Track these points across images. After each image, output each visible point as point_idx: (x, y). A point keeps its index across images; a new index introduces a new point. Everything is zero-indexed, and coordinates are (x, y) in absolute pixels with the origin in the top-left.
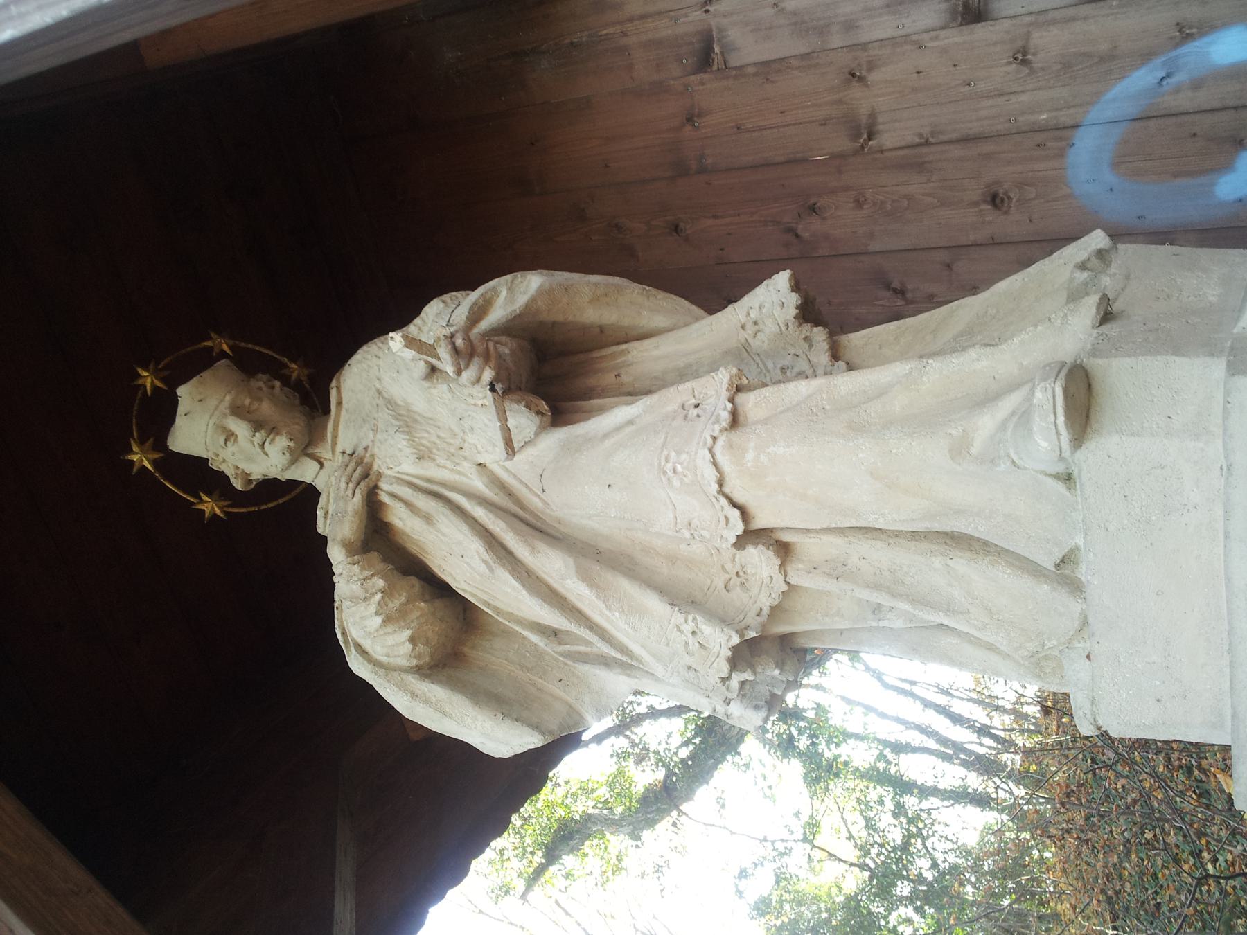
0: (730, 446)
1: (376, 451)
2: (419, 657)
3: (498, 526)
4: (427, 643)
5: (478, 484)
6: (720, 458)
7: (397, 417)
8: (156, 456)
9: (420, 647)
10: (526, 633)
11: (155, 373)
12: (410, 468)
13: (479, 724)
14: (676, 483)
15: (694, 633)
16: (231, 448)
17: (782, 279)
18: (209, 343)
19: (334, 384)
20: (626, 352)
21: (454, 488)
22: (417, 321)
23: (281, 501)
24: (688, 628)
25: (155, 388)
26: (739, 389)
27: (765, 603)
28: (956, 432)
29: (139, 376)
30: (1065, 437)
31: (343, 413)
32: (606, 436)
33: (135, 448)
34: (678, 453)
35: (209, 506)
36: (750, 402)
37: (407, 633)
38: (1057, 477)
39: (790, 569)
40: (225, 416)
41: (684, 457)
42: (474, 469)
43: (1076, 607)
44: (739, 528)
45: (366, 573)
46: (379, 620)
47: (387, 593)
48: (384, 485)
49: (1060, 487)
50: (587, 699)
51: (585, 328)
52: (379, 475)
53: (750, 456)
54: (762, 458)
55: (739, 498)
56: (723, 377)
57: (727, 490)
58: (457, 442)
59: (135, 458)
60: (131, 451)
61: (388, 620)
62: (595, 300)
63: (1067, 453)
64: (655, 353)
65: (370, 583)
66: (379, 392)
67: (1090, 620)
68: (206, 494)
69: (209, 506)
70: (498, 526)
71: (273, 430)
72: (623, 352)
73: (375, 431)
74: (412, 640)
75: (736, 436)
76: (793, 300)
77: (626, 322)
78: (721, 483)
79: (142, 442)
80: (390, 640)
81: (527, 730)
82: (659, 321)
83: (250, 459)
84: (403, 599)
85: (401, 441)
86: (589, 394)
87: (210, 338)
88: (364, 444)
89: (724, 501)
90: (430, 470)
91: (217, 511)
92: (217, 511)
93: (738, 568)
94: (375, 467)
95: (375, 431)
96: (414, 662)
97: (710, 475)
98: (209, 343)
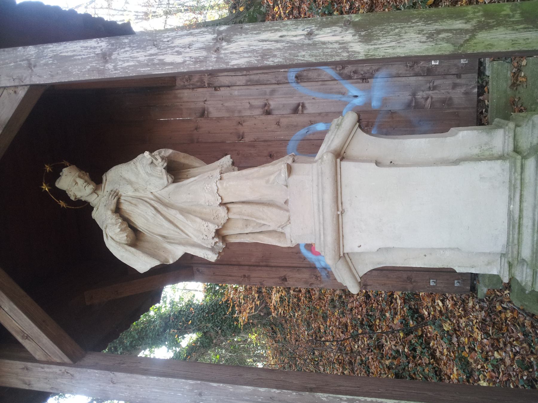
0: (220, 183)
1: (120, 190)
2: (127, 241)
3: (156, 205)
4: (130, 238)
5: (152, 197)
6: (218, 185)
7: (127, 182)
8: (50, 188)
9: (128, 239)
10: (157, 237)
11: (50, 167)
12: (130, 193)
13: (143, 258)
14: (207, 191)
15: (207, 226)
16: (76, 187)
17: (228, 157)
18: (63, 163)
19: (104, 175)
20: (189, 171)
21: (144, 197)
22: (136, 158)
23: (81, 207)
24: (205, 225)
25: (49, 171)
26: (221, 173)
27: (223, 222)
28: (267, 179)
29: (45, 167)
30: (287, 176)
31: (107, 182)
32: (188, 184)
33: (44, 185)
34: (208, 184)
35: (62, 204)
36: (224, 175)
37: (126, 234)
38: (285, 185)
39: (229, 214)
40: (77, 177)
41: (209, 185)
42: (150, 193)
43: (287, 214)
44: (220, 201)
45: (116, 218)
46: (119, 230)
47: (122, 223)
48: (122, 198)
49: (285, 187)
50: (170, 256)
51: (181, 163)
52: (121, 195)
53: (225, 185)
54: (227, 185)
55: (221, 195)
56: (218, 171)
57: (218, 192)
58: (145, 187)
59: (44, 187)
60: (42, 185)
61: (121, 230)
62: (184, 157)
63: (287, 178)
64: (197, 171)
65: (117, 220)
66: (121, 176)
67: (292, 221)
68: (61, 201)
69: (62, 204)
70: (156, 205)
71: (89, 184)
72: (188, 171)
73: (120, 185)
74: (127, 236)
75: (221, 181)
76: (231, 160)
77: (190, 164)
78: (218, 190)
79: (46, 184)
80: (121, 236)
81: (156, 260)
82: (197, 165)
83: (80, 190)
84: (125, 226)
85: (129, 187)
86: (180, 179)
87: (63, 161)
88: (116, 188)
89: (218, 195)
90: (137, 194)
91: (64, 206)
92: (64, 206)
93: (217, 215)
94: (119, 194)
95: (120, 185)
96: (126, 242)
97: (216, 188)
98: (63, 163)
